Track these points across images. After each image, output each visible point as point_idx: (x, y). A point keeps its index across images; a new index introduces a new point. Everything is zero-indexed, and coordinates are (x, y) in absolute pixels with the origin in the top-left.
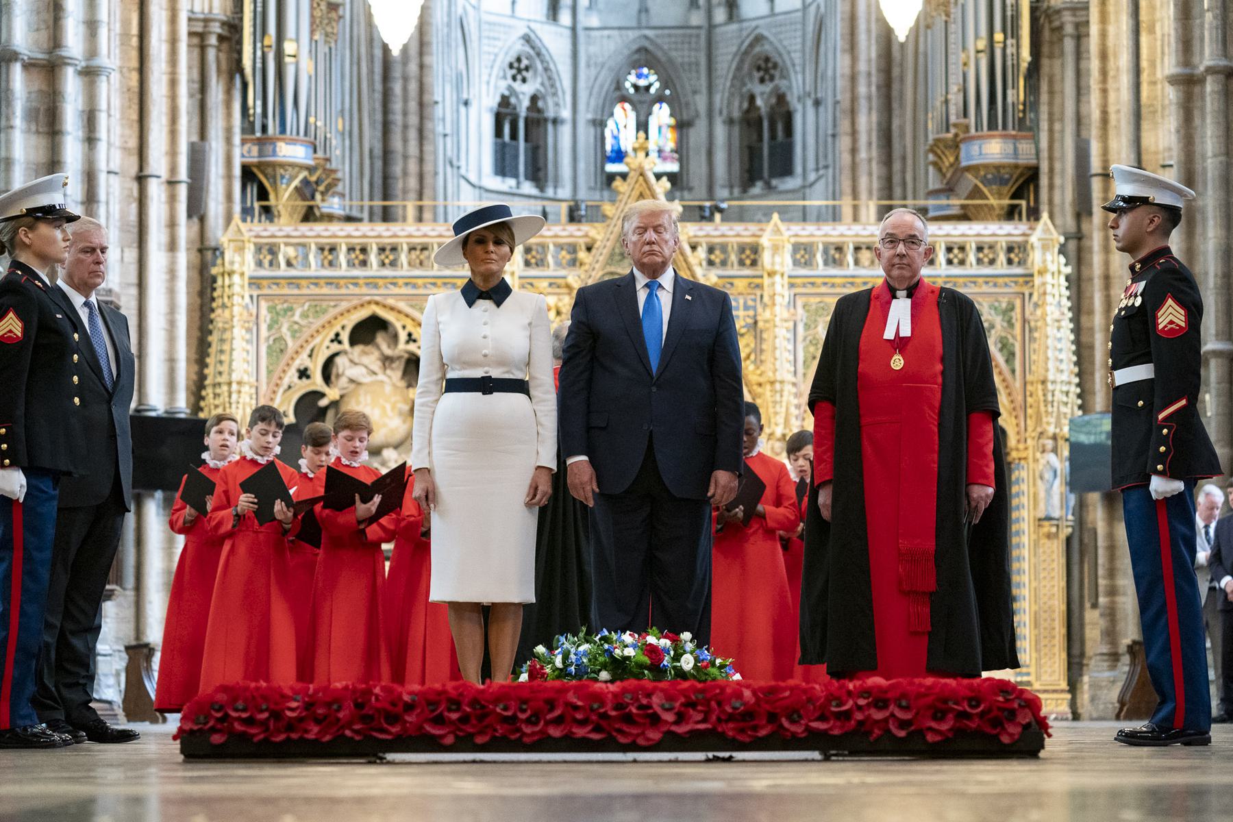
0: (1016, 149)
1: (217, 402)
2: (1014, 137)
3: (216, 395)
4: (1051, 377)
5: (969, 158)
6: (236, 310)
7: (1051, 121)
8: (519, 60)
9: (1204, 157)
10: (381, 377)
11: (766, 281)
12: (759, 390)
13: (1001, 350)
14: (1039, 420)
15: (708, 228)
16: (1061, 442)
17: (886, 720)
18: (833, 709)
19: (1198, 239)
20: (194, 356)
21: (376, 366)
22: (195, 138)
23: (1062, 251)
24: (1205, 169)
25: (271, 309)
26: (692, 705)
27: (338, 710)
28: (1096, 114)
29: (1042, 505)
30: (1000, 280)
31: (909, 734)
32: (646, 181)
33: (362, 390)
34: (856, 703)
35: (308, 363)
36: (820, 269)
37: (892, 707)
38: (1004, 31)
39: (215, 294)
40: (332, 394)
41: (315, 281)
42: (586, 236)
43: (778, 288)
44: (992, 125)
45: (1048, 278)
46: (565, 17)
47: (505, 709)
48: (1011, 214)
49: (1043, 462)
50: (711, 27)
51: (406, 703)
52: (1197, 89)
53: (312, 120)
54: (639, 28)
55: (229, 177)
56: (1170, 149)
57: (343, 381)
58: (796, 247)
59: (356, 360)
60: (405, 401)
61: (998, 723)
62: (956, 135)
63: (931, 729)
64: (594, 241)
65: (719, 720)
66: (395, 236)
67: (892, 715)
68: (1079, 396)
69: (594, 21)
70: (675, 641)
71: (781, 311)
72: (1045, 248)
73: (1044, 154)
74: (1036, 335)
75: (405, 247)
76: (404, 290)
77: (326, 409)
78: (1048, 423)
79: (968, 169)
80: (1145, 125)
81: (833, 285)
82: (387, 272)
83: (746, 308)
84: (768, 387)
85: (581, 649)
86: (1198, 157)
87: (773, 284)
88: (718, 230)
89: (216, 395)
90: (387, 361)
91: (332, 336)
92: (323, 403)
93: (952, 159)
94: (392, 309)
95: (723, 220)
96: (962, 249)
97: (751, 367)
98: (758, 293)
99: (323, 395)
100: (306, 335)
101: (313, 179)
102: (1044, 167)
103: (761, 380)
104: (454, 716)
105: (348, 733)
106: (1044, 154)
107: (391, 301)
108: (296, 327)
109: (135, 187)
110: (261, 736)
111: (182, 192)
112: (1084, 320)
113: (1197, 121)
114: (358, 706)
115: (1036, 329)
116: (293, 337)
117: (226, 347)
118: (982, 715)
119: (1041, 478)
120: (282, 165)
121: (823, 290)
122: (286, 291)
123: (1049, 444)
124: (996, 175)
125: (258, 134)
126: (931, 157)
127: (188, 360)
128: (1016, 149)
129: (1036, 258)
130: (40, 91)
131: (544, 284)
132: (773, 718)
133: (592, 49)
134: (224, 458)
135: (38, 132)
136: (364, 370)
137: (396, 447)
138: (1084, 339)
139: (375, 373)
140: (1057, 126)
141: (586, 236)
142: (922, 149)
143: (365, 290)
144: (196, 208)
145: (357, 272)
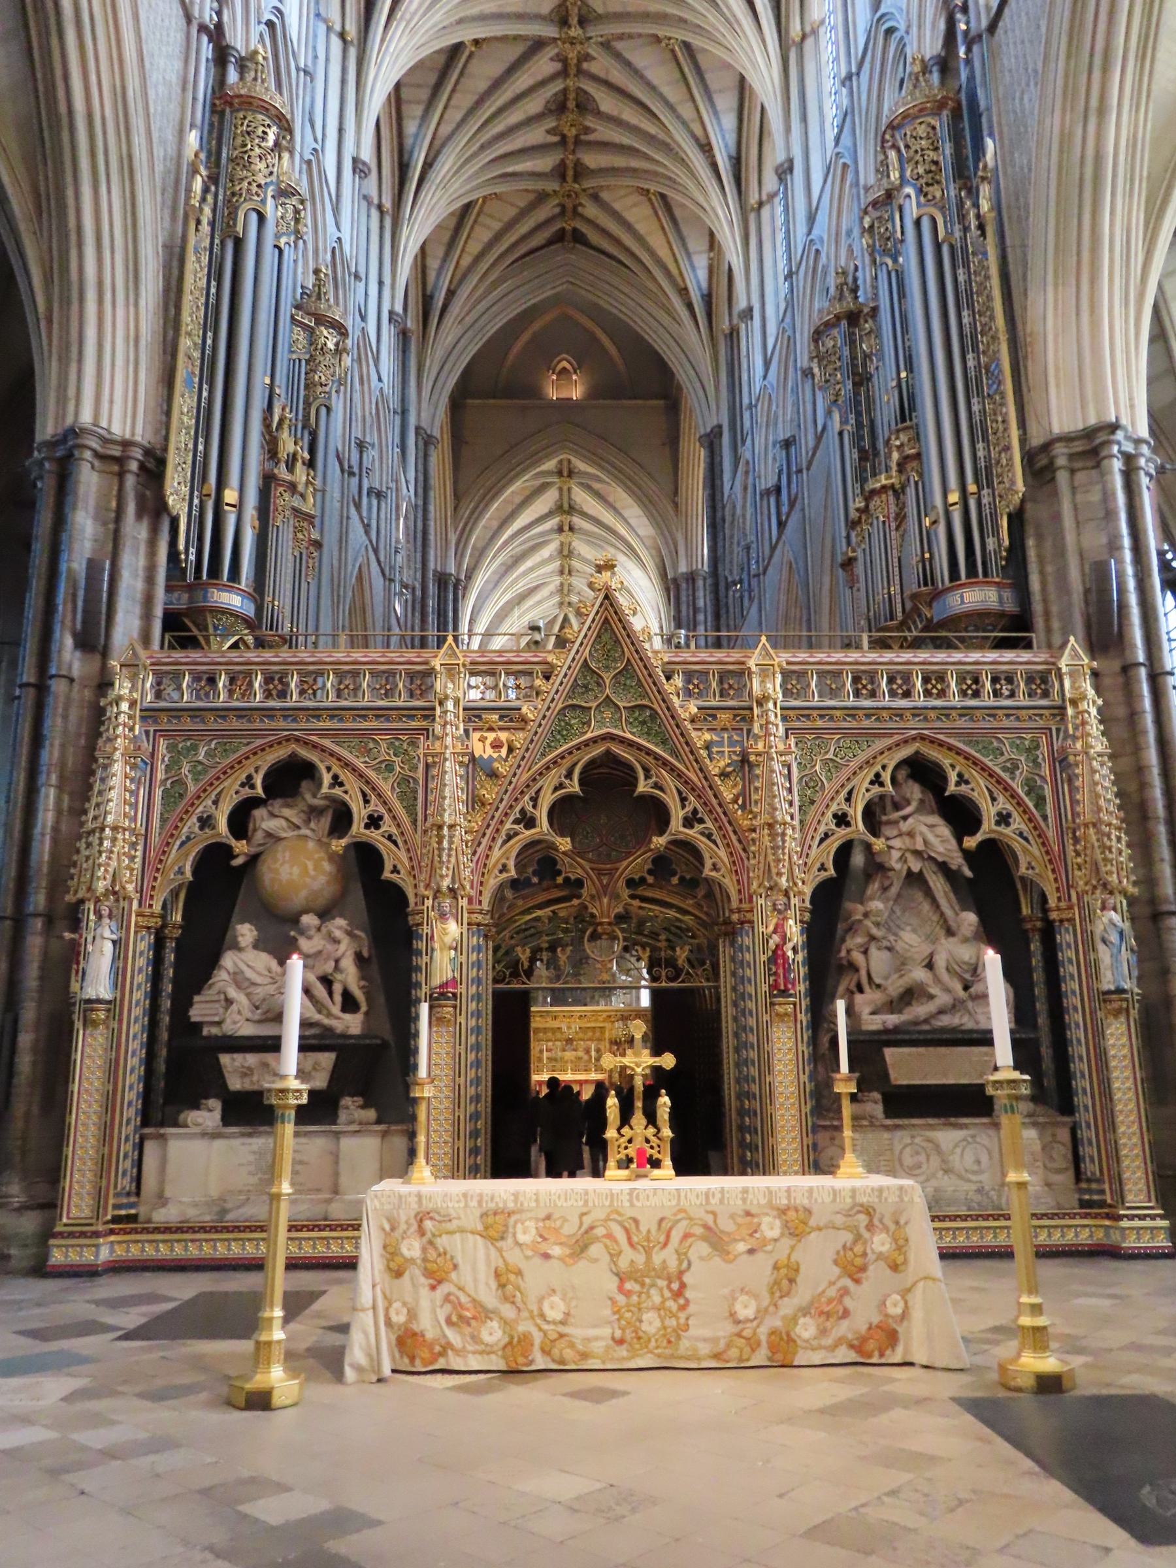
25: (169, 748)
30: (1024, 712)
33: (280, 847)
38: (977, 481)
44: (972, 571)
55: (147, 616)
59: (276, 812)
64: (552, 666)
76: (328, 724)
108: (200, 768)
116: (196, 780)
121: (820, 723)
136: (284, 823)
139: (298, 828)
143: (282, 724)
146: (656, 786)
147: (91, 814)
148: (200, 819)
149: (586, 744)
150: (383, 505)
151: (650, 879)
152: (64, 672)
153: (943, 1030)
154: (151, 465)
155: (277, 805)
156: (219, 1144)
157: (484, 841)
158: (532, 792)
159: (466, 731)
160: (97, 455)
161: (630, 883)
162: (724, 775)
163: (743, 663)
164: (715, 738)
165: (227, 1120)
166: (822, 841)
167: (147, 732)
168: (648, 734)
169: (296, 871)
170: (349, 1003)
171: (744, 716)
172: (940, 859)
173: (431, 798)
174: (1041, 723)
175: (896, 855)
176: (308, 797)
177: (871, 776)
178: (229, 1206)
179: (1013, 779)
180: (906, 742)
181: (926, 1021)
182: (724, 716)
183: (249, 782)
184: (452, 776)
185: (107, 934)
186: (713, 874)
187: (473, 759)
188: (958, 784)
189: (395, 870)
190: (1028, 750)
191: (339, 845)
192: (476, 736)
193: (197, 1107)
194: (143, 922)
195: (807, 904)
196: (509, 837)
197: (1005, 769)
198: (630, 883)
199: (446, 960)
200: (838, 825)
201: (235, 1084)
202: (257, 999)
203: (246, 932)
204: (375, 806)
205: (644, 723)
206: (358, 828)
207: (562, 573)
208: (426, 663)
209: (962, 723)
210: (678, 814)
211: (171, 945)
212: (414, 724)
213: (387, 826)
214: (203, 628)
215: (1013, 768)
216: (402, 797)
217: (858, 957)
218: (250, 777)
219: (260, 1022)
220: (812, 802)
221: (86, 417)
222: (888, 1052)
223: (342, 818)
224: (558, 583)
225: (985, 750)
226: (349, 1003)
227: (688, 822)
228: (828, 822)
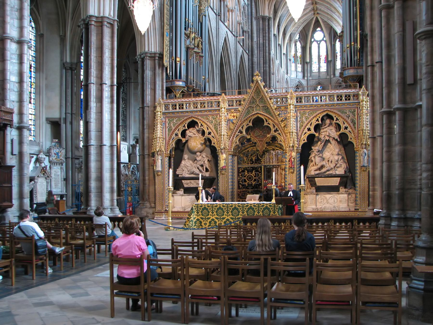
8: (298, 85)
14: (361, 140)
30: (351, 104)
46: (306, 78)
50: (331, 78)
54: (319, 79)
55: (162, 90)
64: (245, 99)
69: (311, 79)
78: (364, 141)
90: (198, 131)
116: (174, 126)
119: (362, 155)
121: (304, 108)
123: (364, 146)
133: (311, 83)
136: (192, 134)
147: (155, 135)
148: (175, 134)
149: (253, 115)
150: (233, 13)
151: (271, 142)
152: (147, 105)
153: (328, 175)
154: (161, 56)
155: (191, 129)
156: (183, 197)
159: (227, 114)
160: (149, 57)
161: (267, 143)
163: (287, 96)
164: (281, 113)
165: (184, 193)
166: (304, 134)
167: (164, 117)
168: (267, 112)
169: (195, 144)
170: (207, 170)
171: (286, 108)
172: (333, 137)
174: (356, 106)
176: (197, 128)
177: (316, 119)
178: (186, 208)
179: (349, 119)
180: (324, 111)
181: (325, 172)
182: (283, 108)
183: (184, 126)
184: (224, 124)
185: (160, 158)
186: (280, 142)
188: (336, 120)
189: (214, 143)
190: (353, 112)
193: (179, 190)
195: (300, 148)
197: (347, 117)
198: (267, 143)
199: (223, 162)
200: (308, 131)
201: (186, 186)
202: (189, 170)
203: (186, 156)
205: (266, 110)
206: (206, 134)
207: (313, 4)
208: (218, 99)
209: (337, 107)
210: (273, 130)
211: (172, 159)
212: (217, 113)
213: (212, 134)
214: (175, 90)
215: (348, 117)
217: (313, 159)
218: (184, 125)
219: (189, 174)
220: (302, 126)
221: (147, 50)
222: (316, 179)
223: (203, 133)
224: (312, 7)
225: (343, 112)
226: (207, 170)
227: (275, 131)
228: (306, 130)
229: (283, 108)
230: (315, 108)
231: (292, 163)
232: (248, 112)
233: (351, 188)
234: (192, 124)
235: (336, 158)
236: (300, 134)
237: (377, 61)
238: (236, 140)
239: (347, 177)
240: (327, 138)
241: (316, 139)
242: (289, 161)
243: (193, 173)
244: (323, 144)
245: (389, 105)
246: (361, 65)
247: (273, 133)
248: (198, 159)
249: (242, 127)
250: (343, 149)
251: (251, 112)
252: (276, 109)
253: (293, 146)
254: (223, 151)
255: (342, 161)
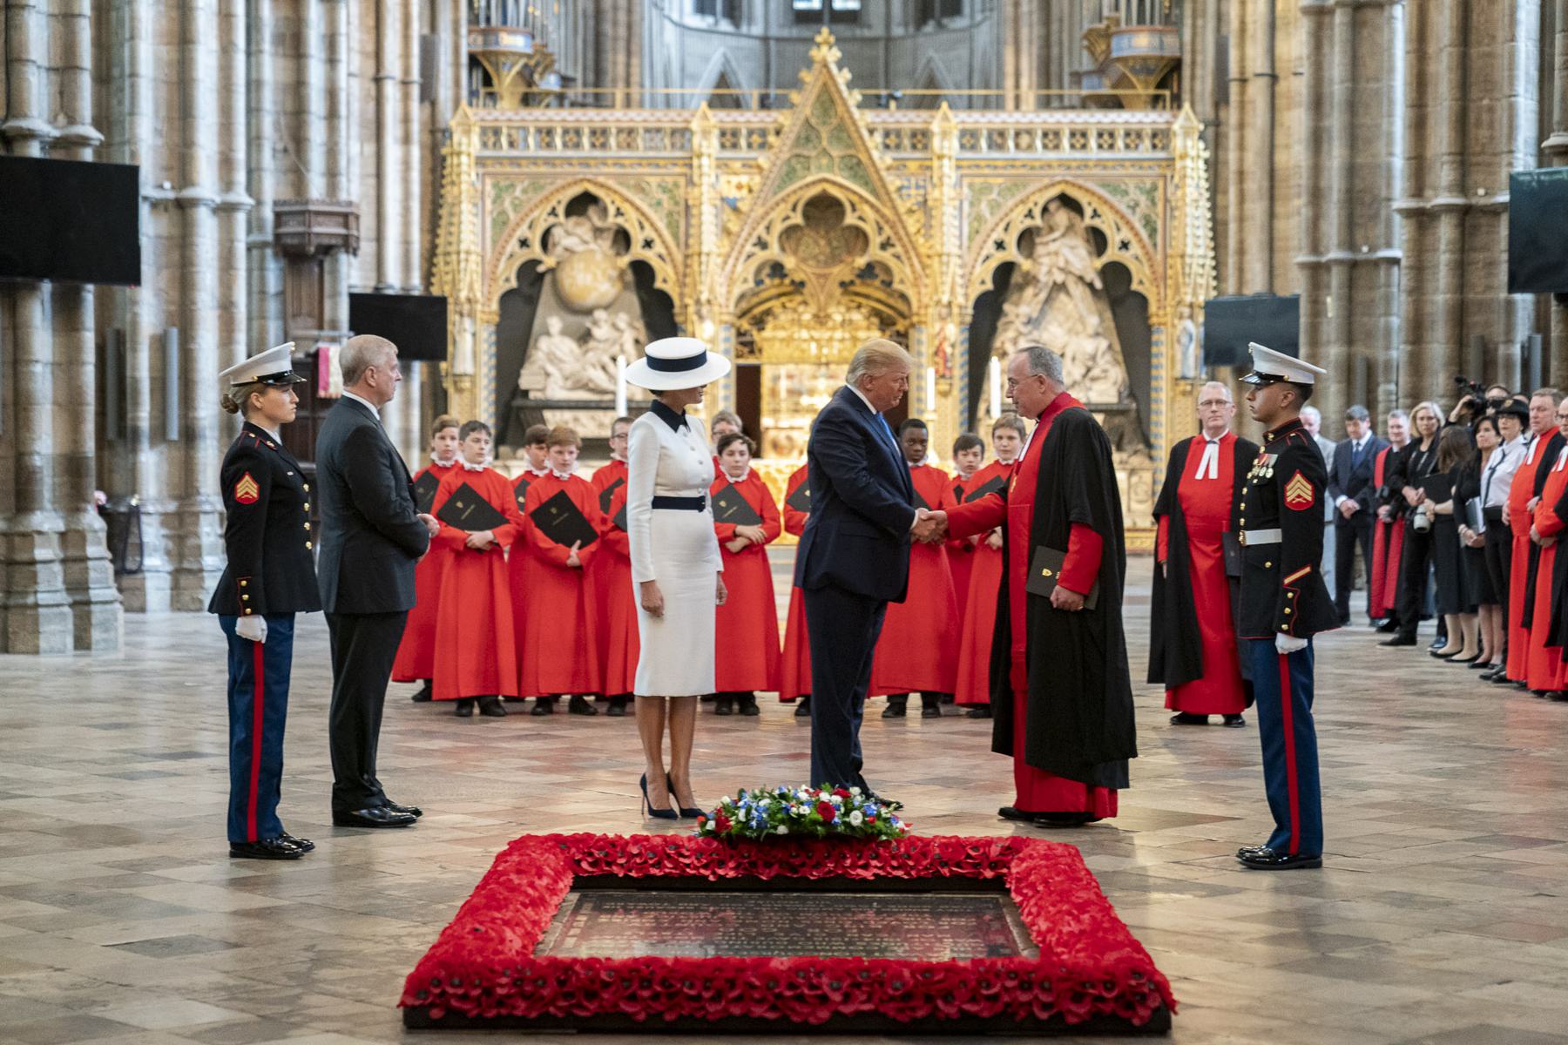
0: (1162, 42)
1: (448, 269)
2: (1160, 32)
3: (447, 263)
4: (1189, 251)
5: (1121, 49)
6: (464, 187)
7: (1194, 18)
9: (1331, 80)
10: (593, 246)
11: (935, 163)
12: (928, 261)
13: (1145, 226)
14: (1177, 290)
15: (883, 116)
16: (1197, 310)
17: (1029, 1004)
18: (985, 992)
19: (1324, 156)
20: (427, 227)
21: (588, 236)
22: (426, 31)
23: (1202, 137)
24: (1332, 93)
25: (495, 186)
26: (857, 985)
27: (543, 987)
28: (1234, 24)
29: (1178, 367)
30: (1146, 164)
31: (1051, 1018)
32: (829, 72)
33: (575, 258)
34: (1003, 987)
35: (528, 234)
36: (984, 151)
37: (1036, 991)
39: (446, 172)
40: (549, 262)
41: (534, 161)
42: (775, 121)
43: (946, 170)
44: (1141, 20)
45: (1189, 163)
47: (692, 987)
48: (1155, 101)
49: (1180, 327)
51: (603, 981)
52: (1327, 19)
53: (530, 10)
55: (457, 64)
56: (1300, 58)
57: (559, 250)
58: (963, 133)
60: (615, 267)
61: (1130, 1006)
62: (1108, 27)
63: (1070, 1012)
64: (782, 126)
65: (882, 1001)
66: (605, 120)
67: (1036, 997)
68: (1215, 268)
70: (846, 797)
71: (948, 191)
72: (1187, 134)
73: (1188, 48)
74: (1177, 213)
75: (614, 131)
77: (541, 276)
79: (1118, 59)
80: (1279, 35)
81: (996, 167)
82: (598, 153)
83: (918, 187)
84: (936, 259)
85: (762, 803)
86: (1326, 84)
87: (941, 167)
88: (894, 117)
89: (447, 263)
90: (598, 232)
91: (549, 209)
92: (541, 269)
93: (1104, 47)
94: (602, 186)
95: (898, 107)
96: (1111, 135)
97: (921, 240)
98: (928, 173)
99: (539, 262)
100: (526, 209)
101: (532, 63)
102: (1187, 59)
103: (930, 252)
104: (646, 994)
105: (552, 1009)
106: (1188, 48)
107: (601, 179)
109: (372, 87)
110: (475, 1012)
111: (415, 91)
112: (1220, 198)
113: (1326, 49)
114: (562, 983)
115: (1177, 208)
117: (455, 220)
118: (1116, 999)
119: (1179, 341)
120: (504, 54)
121: (986, 171)
122: (508, 169)
123: (1186, 311)
124: (1143, 65)
125: (483, 25)
126: (1085, 43)
127: (422, 230)
128: (1162, 42)
129: (1178, 143)
130: (287, 18)
131: (737, 165)
132: (929, 999)
134: (447, 459)
135: (285, 55)
137: (607, 307)
138: (1220, 216)
140: (1200, 22)
141: (775, 121)
142: (1078, 35)
143: (577, 169)
144: (428, 94)
145: (570, 153)
146: (861, 218)
149: (807, 186)
151: (858, 281)
157: (731, 261)
158: (765, 223)
161: (843, 284)
162: (911, 211)
173: (692, 231)
175: (1044, 269)
180: (1053, 185)
187: (723, 199)
189: (665, 281)
191: (625, 261)
192: (723, 178)
194: (485, 317)
195: (970, 311)
196: (749, 257)
198: (843, 284)
204: (649, 233)
210: (876, 240)
213: (658, 247)
216: (669, 225)
225: (1115, 190)
228: (990, 247)
229: (913, 166)
230: (1022, 171)
231: (946, 361)
232: (790, 175)
233: (1136, 452)
234: (582, 204)
235: (1089, 346)
236: (969, 259)
237: (1259, 71)
238: (745, 272)
239: (1123, 412)
240: (1059, 278)
241: (1016, 278)
242: (936, 353)
243: (585, 387)
244: (1043, 296)
245: (1315, 246)
246: (1173, 19)
247: (874, 253)
248: (597, 332)
249: (768, 228)
250: (1108, 315)
251: (800, 173)
252: (888, 168)
253: (950, 304)
254: (705, 310)
255: (1108, 357)
